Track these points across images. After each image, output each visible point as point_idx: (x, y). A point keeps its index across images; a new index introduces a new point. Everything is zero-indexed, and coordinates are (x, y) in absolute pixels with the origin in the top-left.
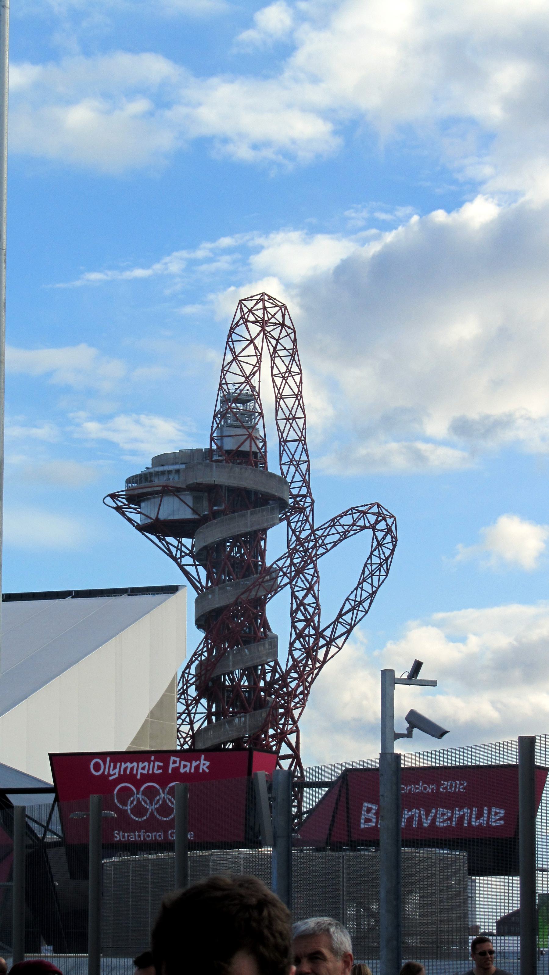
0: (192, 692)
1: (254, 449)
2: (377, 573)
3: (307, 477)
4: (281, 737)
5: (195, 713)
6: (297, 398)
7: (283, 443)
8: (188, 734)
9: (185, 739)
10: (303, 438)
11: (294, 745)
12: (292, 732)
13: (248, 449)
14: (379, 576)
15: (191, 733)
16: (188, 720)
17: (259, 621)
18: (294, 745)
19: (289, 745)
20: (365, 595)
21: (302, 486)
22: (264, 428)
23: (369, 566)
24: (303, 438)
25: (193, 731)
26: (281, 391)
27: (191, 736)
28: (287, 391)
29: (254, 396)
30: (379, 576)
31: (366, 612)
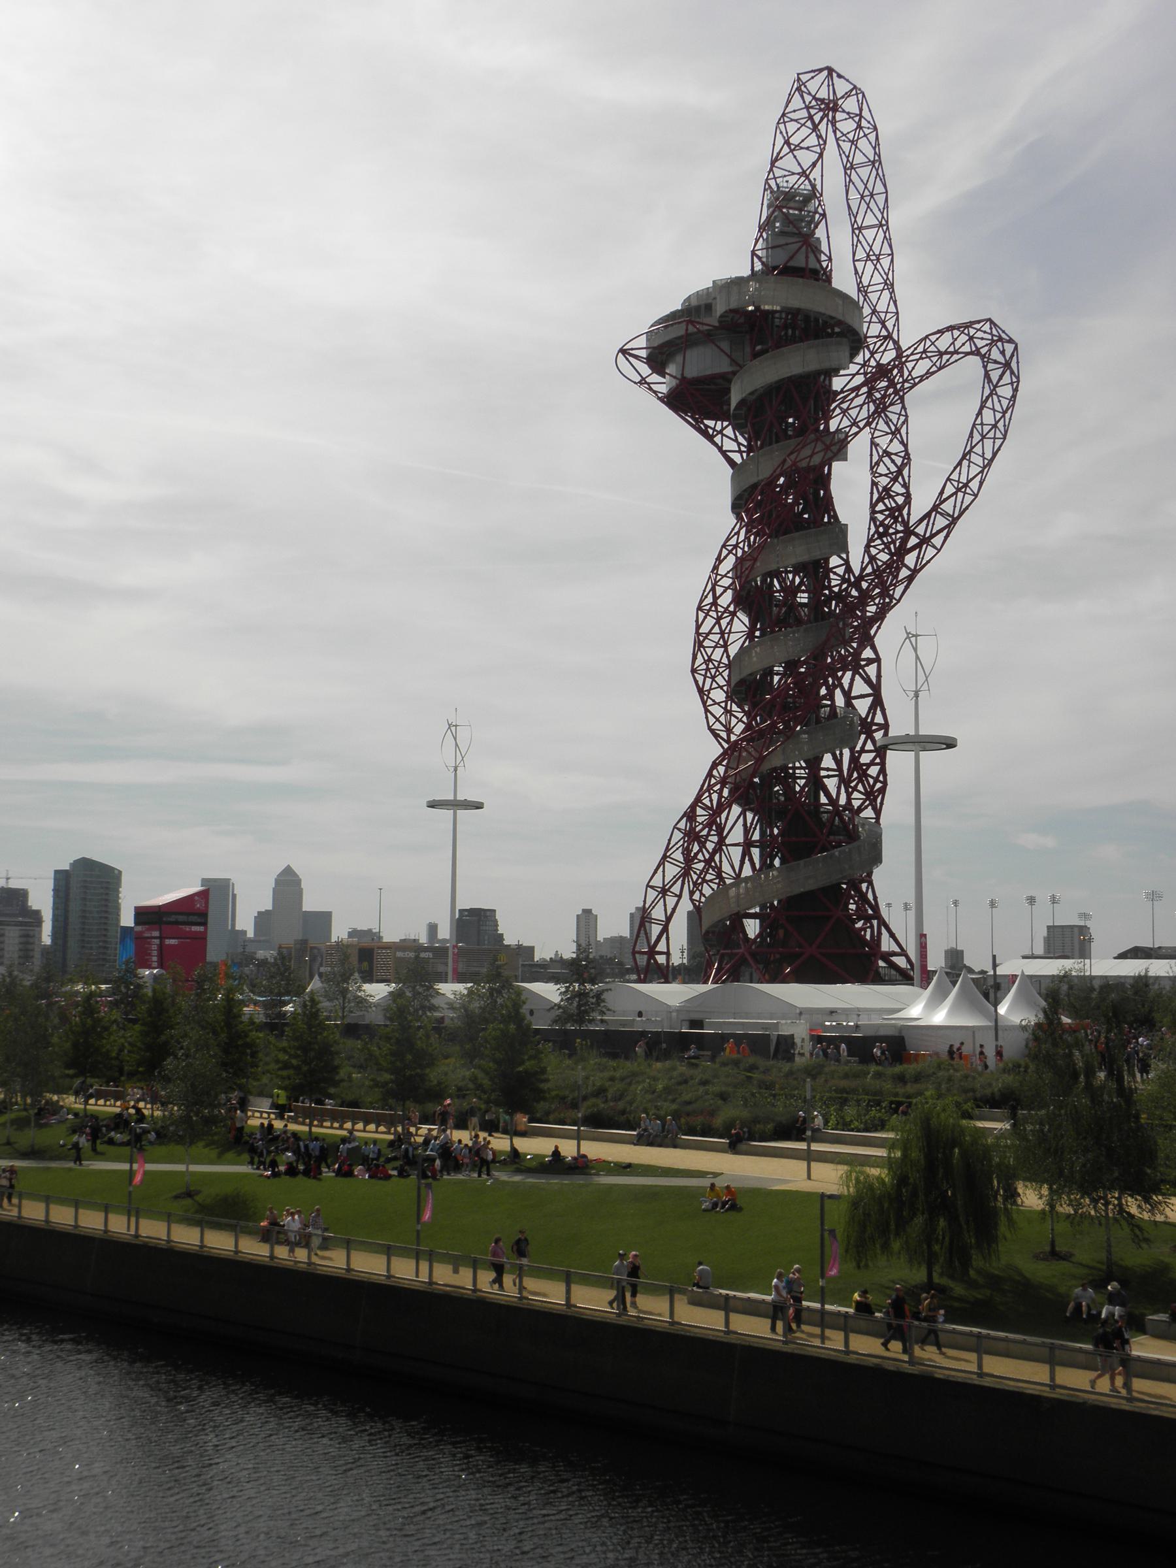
0: (726, 599)
1: (812, 264)
2: (991, 435)
3: (890, 276)
4: (856, 666)
5: (730, 632)
6: (874, 166)
7: (857, 232)
8: (720, 662)
9: (717, 668)
10: (884, 222)
11: (874, 680)
12: (870, 661)
13: (803, 265)
14: (995, 438)
15: (725, 660)
16: (721, 642)
17: (822, 492)
18: (874, 680)
19: (867, 681)
20: (975, 470)
21: (883, 289)
22: (828, 237)
23: (979, 427)
24: (884, 222)
25: (728, 657)
26: (851, 159)
27: (729, 666)
28: (859, 158)
29: (814, 194)
30: (995, 438)
31: (976, 496)
